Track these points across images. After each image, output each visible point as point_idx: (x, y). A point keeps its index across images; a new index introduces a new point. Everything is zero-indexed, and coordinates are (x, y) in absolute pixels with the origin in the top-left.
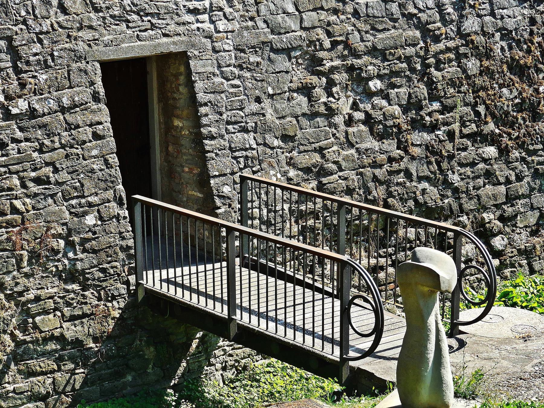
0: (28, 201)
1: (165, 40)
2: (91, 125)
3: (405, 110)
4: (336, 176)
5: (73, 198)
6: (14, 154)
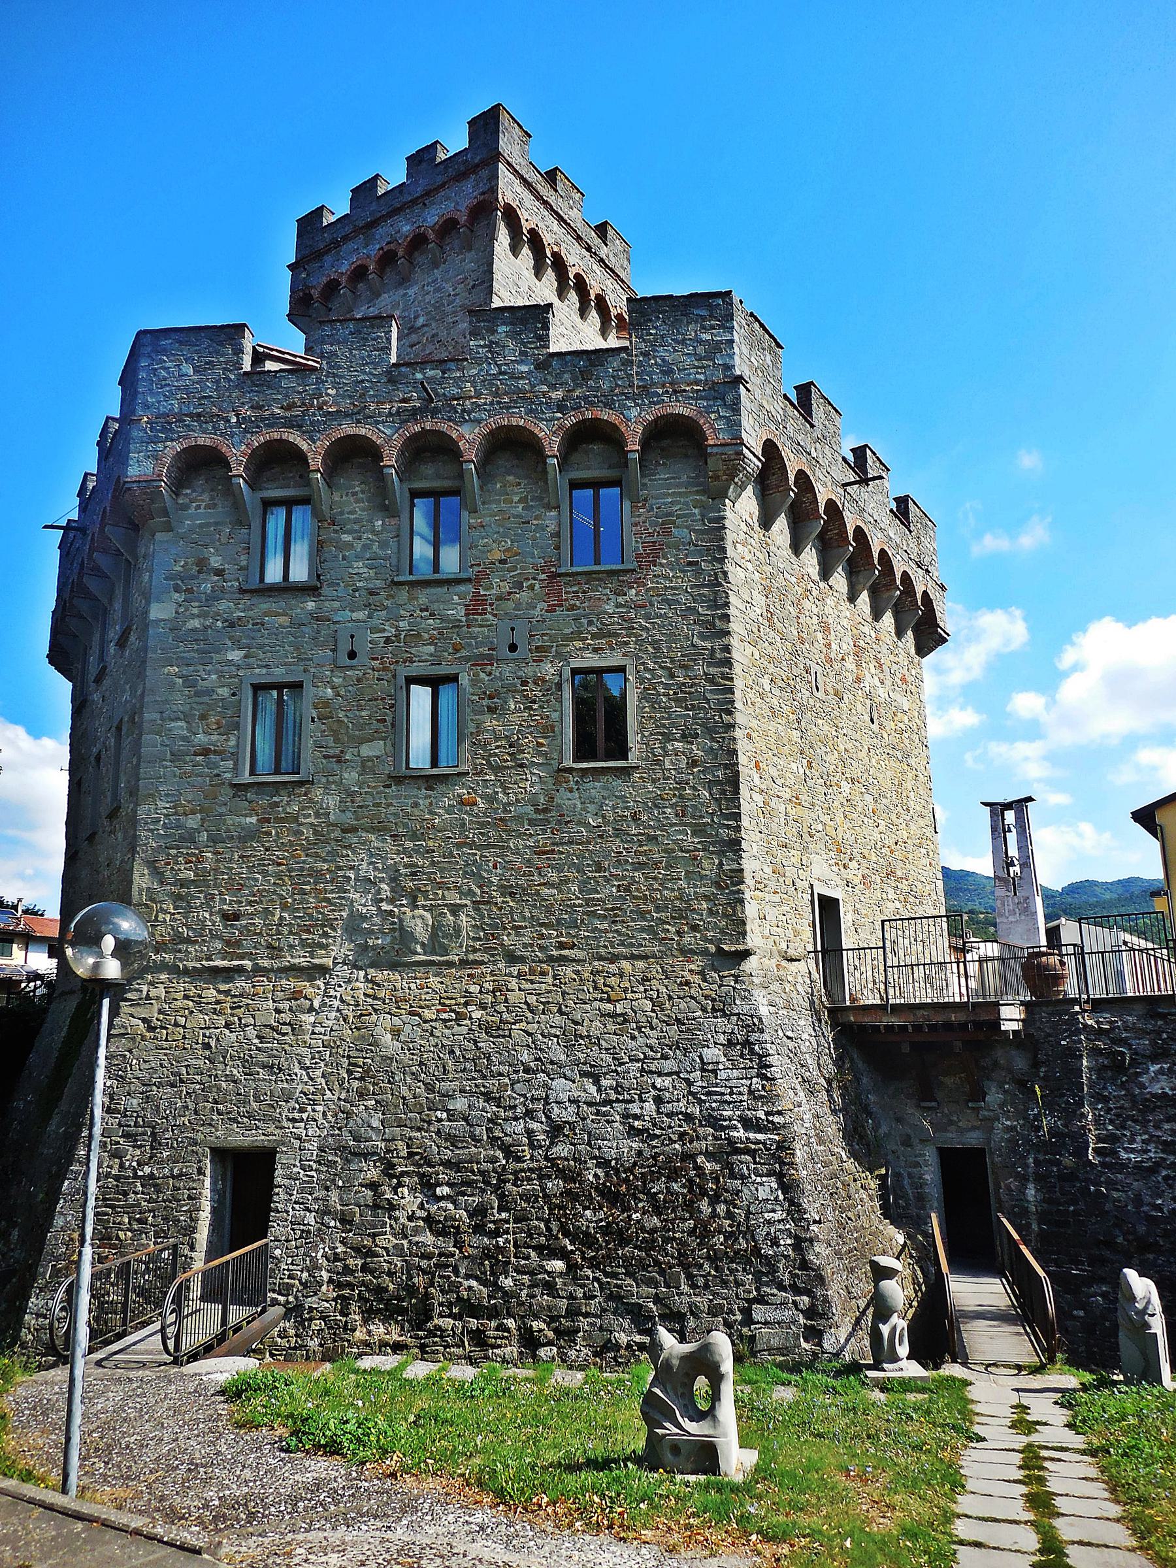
0: (129, 1234)
1: (263, 1137)
2: (188, 1190)
3: (471, 1216)
4: (382, 1259)
5: (160, 1237)
6: (130, 1201)
